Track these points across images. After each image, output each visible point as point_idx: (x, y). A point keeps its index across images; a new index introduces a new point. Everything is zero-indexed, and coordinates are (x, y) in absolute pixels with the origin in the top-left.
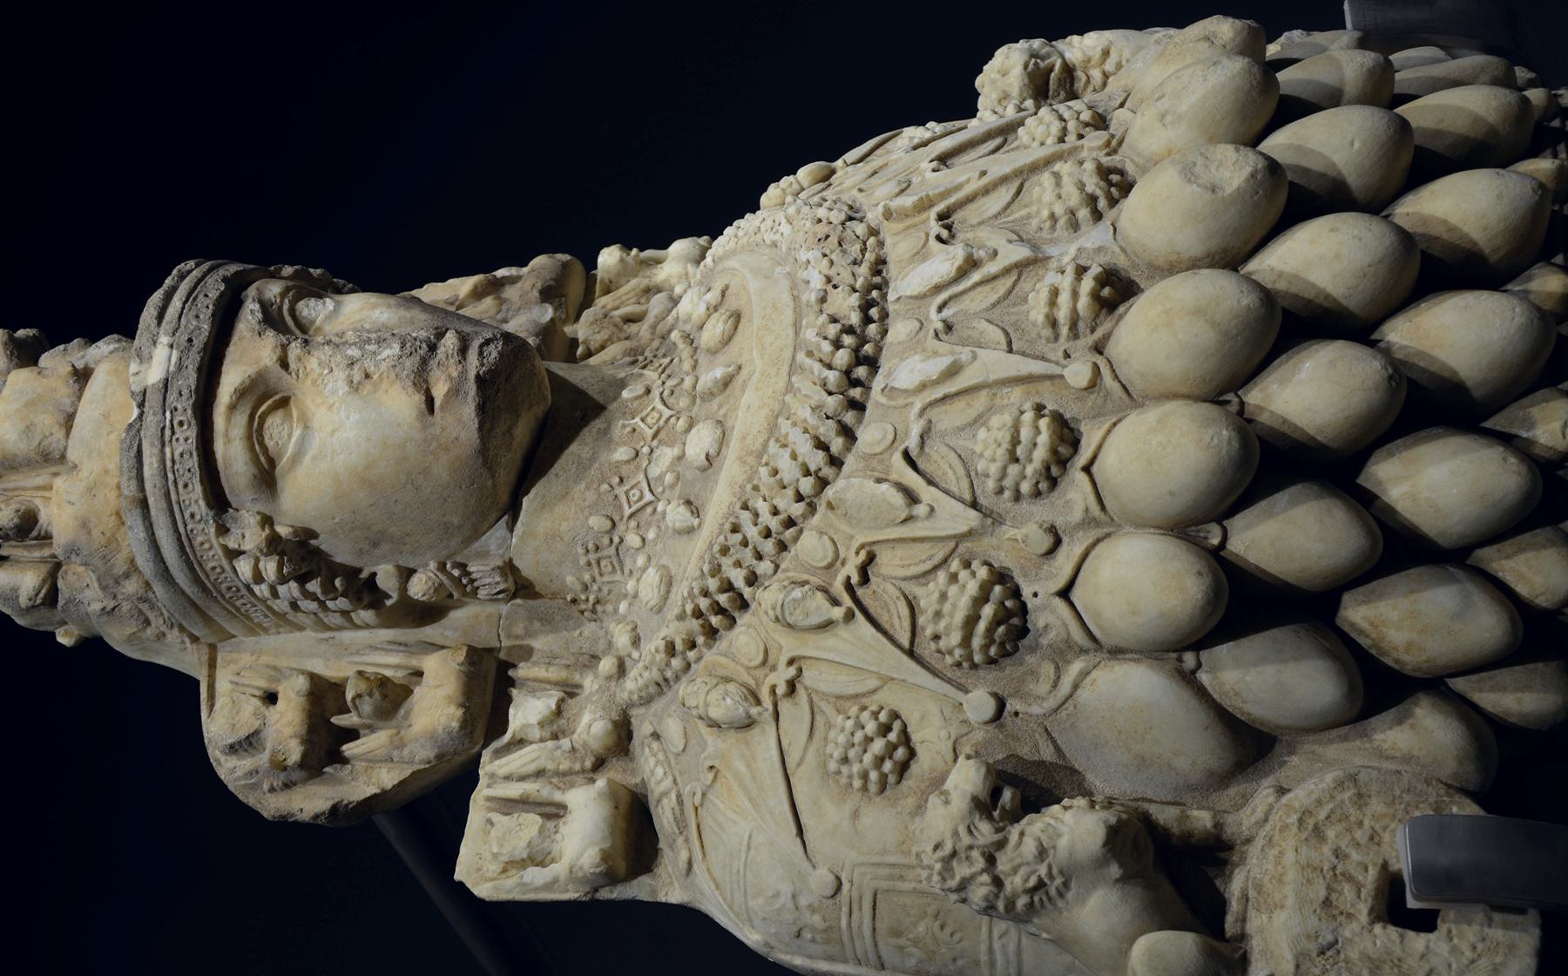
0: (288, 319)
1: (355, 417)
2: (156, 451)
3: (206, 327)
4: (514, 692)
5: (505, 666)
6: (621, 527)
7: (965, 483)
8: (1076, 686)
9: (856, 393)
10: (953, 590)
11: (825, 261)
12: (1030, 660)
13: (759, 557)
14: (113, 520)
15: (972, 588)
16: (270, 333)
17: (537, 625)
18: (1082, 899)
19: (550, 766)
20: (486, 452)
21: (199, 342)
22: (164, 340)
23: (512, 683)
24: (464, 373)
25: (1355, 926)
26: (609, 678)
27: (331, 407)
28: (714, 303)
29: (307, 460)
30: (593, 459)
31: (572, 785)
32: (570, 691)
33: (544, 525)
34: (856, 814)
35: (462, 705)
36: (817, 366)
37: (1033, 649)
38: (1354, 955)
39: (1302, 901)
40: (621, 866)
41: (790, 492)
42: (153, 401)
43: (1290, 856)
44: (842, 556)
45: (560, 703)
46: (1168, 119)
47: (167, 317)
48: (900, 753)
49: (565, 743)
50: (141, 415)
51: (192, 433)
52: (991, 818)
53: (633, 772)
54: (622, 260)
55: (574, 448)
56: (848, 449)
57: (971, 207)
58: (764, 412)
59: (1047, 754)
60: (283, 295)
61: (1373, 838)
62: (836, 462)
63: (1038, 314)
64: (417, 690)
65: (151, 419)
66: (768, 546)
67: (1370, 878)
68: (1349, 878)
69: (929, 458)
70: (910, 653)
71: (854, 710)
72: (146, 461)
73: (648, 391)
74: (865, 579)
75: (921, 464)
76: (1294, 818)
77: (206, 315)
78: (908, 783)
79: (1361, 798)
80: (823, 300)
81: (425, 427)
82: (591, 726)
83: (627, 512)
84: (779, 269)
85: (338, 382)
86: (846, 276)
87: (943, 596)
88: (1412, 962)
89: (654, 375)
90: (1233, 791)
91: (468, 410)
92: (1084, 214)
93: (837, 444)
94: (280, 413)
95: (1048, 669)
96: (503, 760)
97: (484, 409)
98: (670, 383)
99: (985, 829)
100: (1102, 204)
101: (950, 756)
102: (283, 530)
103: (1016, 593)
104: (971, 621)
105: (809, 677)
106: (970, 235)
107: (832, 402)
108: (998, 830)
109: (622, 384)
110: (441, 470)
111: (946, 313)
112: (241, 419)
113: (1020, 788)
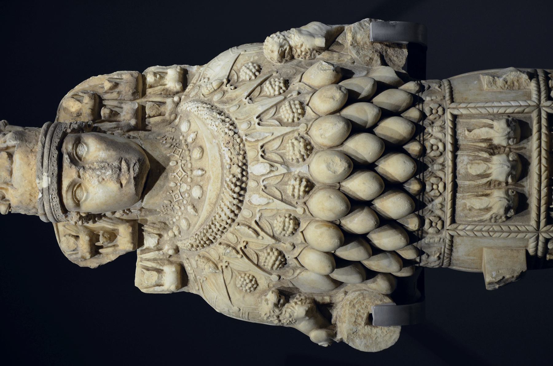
0: (76, 157)
1: (101, 191)
2: (48, 204)
3: (56, 169)
4: (144, 233)
5: (141, 226)
6: (173, 203)
7: (271, 231)
8: (298, 275)
9: (241, 198)
10: (269, 258)
11: (230, 154)
12: (287, 269)
13: (216, 234)
14: (29, 201)
15: (274, 258)
16: (73, 166)
17: (148, 213)
18: (299, 323)
19: (158, 257)
20: (137, 194)
21: (56, 173)
22: (45, 174)
23: (143, 230)
24: (130, 177)
25: (361, 327)
26: (172, 237)
27: (94, 187)
28: (194, 138)
29: (88, 200)
30: (164, 185)
31: (164, 265)
32: (160, 236)
33: (152, 201)
34: (244, 297)
35: (132, 243)
36: (231, 192)
37: (288, 267)
38: (360, 334)
39: (349, 322)
40: (180, 286)
41: (225, 223)
42: (46, 193)
43: (347, 311)
44: (239, 240)
45: (159, 240)
46: (323, 136)
47: (44, 167)
48: (255, 286)
49: (161, 252)
50: (43, 196)
51: (58, 200)
52: (278, 307)
53: (180, 258)
54: (155, 80)
55: (158, 182)
56: (239, 212)
57: (269, 143)
58: (215, 193)
59: (291, 286)
60: (73, 148)
61: (366, 307)
62: (236, 215)
63: (289, 192)
64: (118, 237)
65: (46, 197)
66: (219, 233)
67: (365, 316)
68: (360, 316)
69: (261, 223)
70: (257, 265)
71: (243, 275)
72: (45, 205)
73: (177, 163)
74: (245, 247)
75: (259, 223)
76: (348, 303)
77: (55, 164)
78: (257, 291)
79: (364, 298)
80: (230, 168)
81: (120, 191)
82: (168, 249)
83: (175, 200)
84: (214, 140)
85: (95, 181)
86: (235, 160)
87: (266, 259)
88: (373, 335)
89: (178, 157)
90: (334, 291)
91: (132, 186)
92: (301, 160)
93: (236, 212)
94: (79, 188)
95: (292, 271)
96: (144, 255)
97: (136, 185)
98: (183, 162)
99: (277, 310)
100: (305, 157)
101: (267, 286)
102: (84, 215)
103: (284, 256)
104: (274, 264)
105: (231, 265)
106: (270, 155)
107: (235, 202)
108: (280, 311)
109: (168, 159)
110: (125, 199)
111: (265, 183)
112: (70, 193)
113: (285, 295)
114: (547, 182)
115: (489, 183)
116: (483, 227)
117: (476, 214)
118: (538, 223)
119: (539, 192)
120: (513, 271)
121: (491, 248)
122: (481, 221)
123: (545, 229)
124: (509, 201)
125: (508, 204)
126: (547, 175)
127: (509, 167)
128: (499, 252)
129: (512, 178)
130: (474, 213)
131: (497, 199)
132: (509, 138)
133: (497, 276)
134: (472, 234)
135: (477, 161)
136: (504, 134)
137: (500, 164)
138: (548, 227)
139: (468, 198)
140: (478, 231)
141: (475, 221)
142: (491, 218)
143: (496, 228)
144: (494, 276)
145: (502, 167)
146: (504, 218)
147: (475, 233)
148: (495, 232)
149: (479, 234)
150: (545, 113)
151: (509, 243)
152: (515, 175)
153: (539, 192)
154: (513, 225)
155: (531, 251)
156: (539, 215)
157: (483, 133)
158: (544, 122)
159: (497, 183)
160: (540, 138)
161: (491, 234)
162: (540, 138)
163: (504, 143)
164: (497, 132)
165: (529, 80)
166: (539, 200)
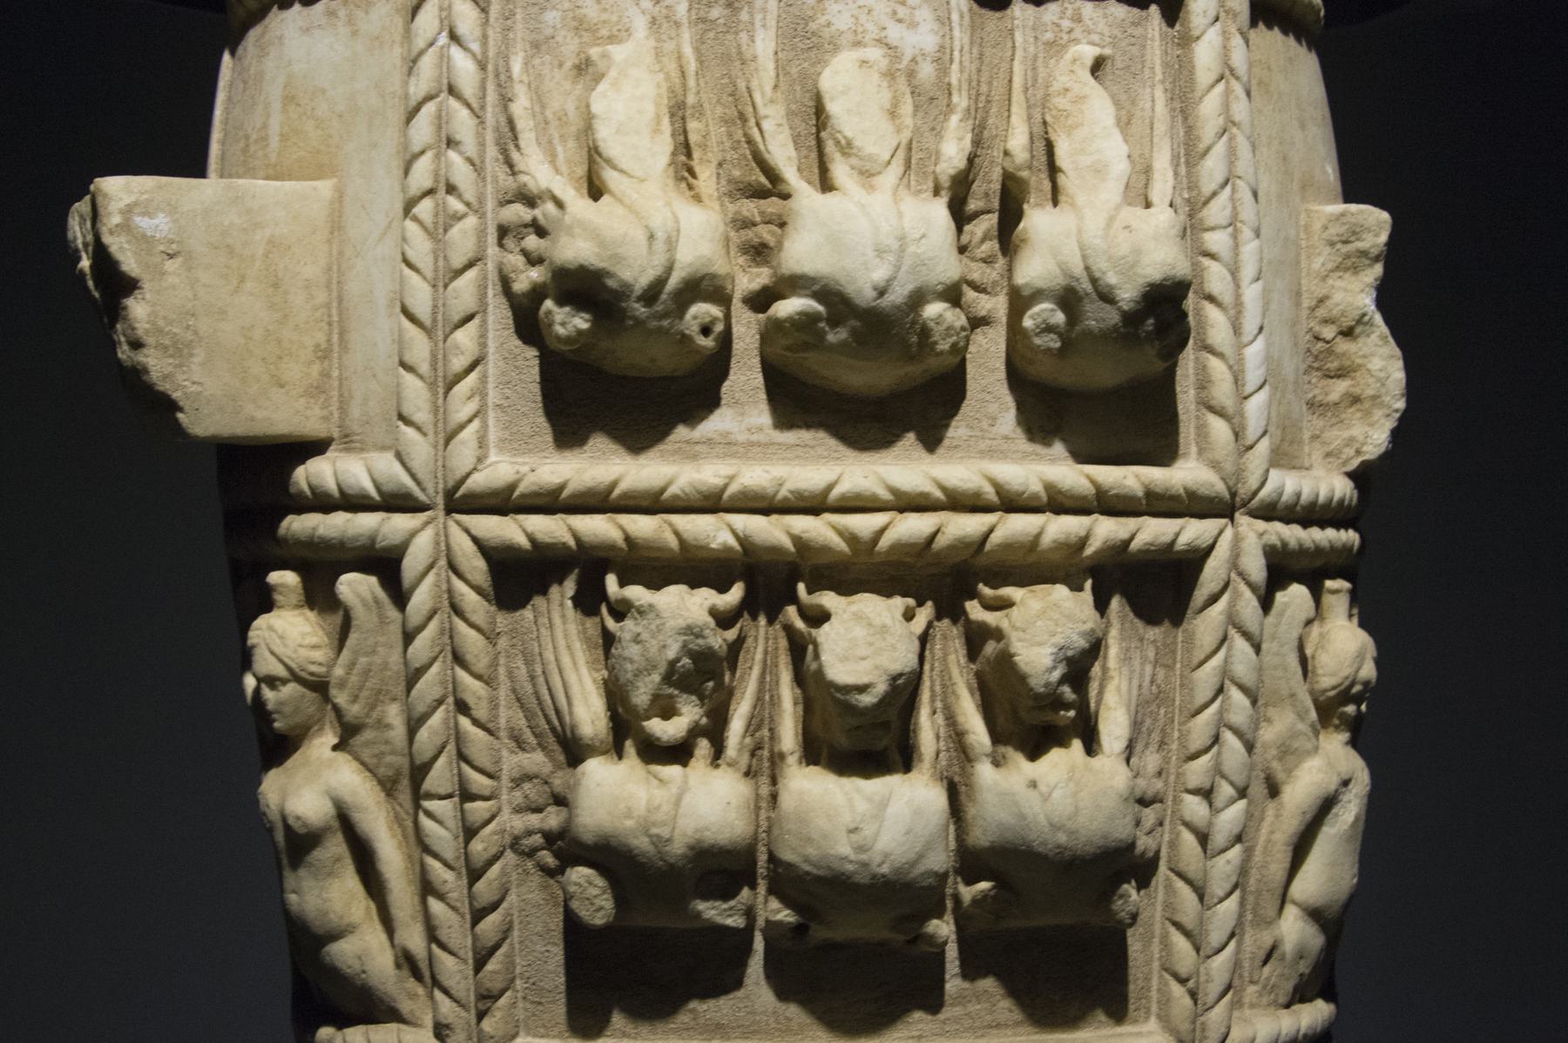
114: (776, 550)
115: (770, 186)
116: (470, 147)
117: (555, 105)
118: (503, 502)
119: (711, 503)
120: (179, 350)
121: (336, 224)
122: (510, 133)
123: (464, 547)
124: (652, 294)
125: (623, 292)
126: (826, 549)
127: (882, 293)
128: (312, 270)
129: (805, 322)
130: (563, 95)
131: (659, 219)
132: (1068, 299)
133: (144, 241)
134: (418, 88)
135: (907, 107)
136: (1100, 265)
137: (902, 238)
138: (477, 566)
139: (658, 54)
140: (440, 120)
141: (505, 101)
142: (530, 201)
143: (463, 239)
144: (143, 222)
145: (880, 252)
146: (527, 278)
147: (429, 109)
148: (438, 231)
149: (422, 130)
150: (1205, 541)
151: (378, 333)
152: (818, 342)
153: (711, 503)
154: (483, 335)
155: (318, 472)
156: (550, 502)
157: (1096, 141)
158: (1151, 531)
159: (766, 233)
160: (1058, 503)
161: (425, 208)
162: (1058, 503)
163: (1034, 269)
164: (1111, 220)
165: (1354, 464)
166: (652, 503)
